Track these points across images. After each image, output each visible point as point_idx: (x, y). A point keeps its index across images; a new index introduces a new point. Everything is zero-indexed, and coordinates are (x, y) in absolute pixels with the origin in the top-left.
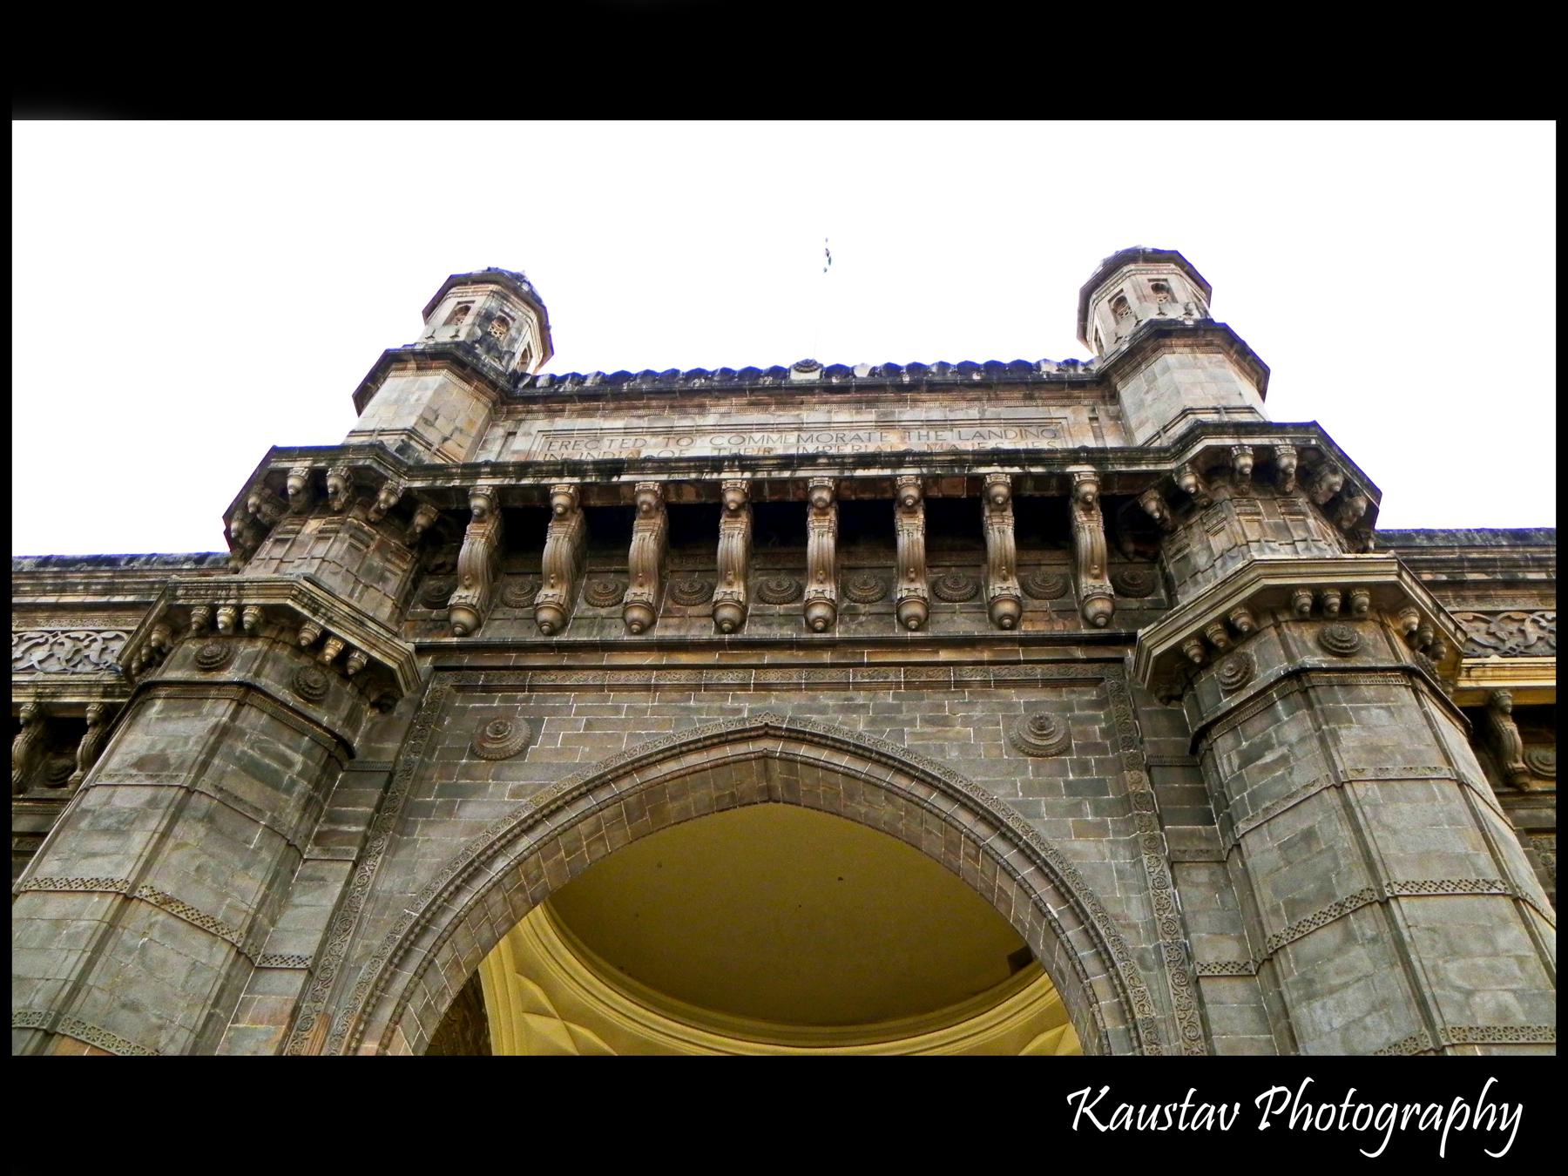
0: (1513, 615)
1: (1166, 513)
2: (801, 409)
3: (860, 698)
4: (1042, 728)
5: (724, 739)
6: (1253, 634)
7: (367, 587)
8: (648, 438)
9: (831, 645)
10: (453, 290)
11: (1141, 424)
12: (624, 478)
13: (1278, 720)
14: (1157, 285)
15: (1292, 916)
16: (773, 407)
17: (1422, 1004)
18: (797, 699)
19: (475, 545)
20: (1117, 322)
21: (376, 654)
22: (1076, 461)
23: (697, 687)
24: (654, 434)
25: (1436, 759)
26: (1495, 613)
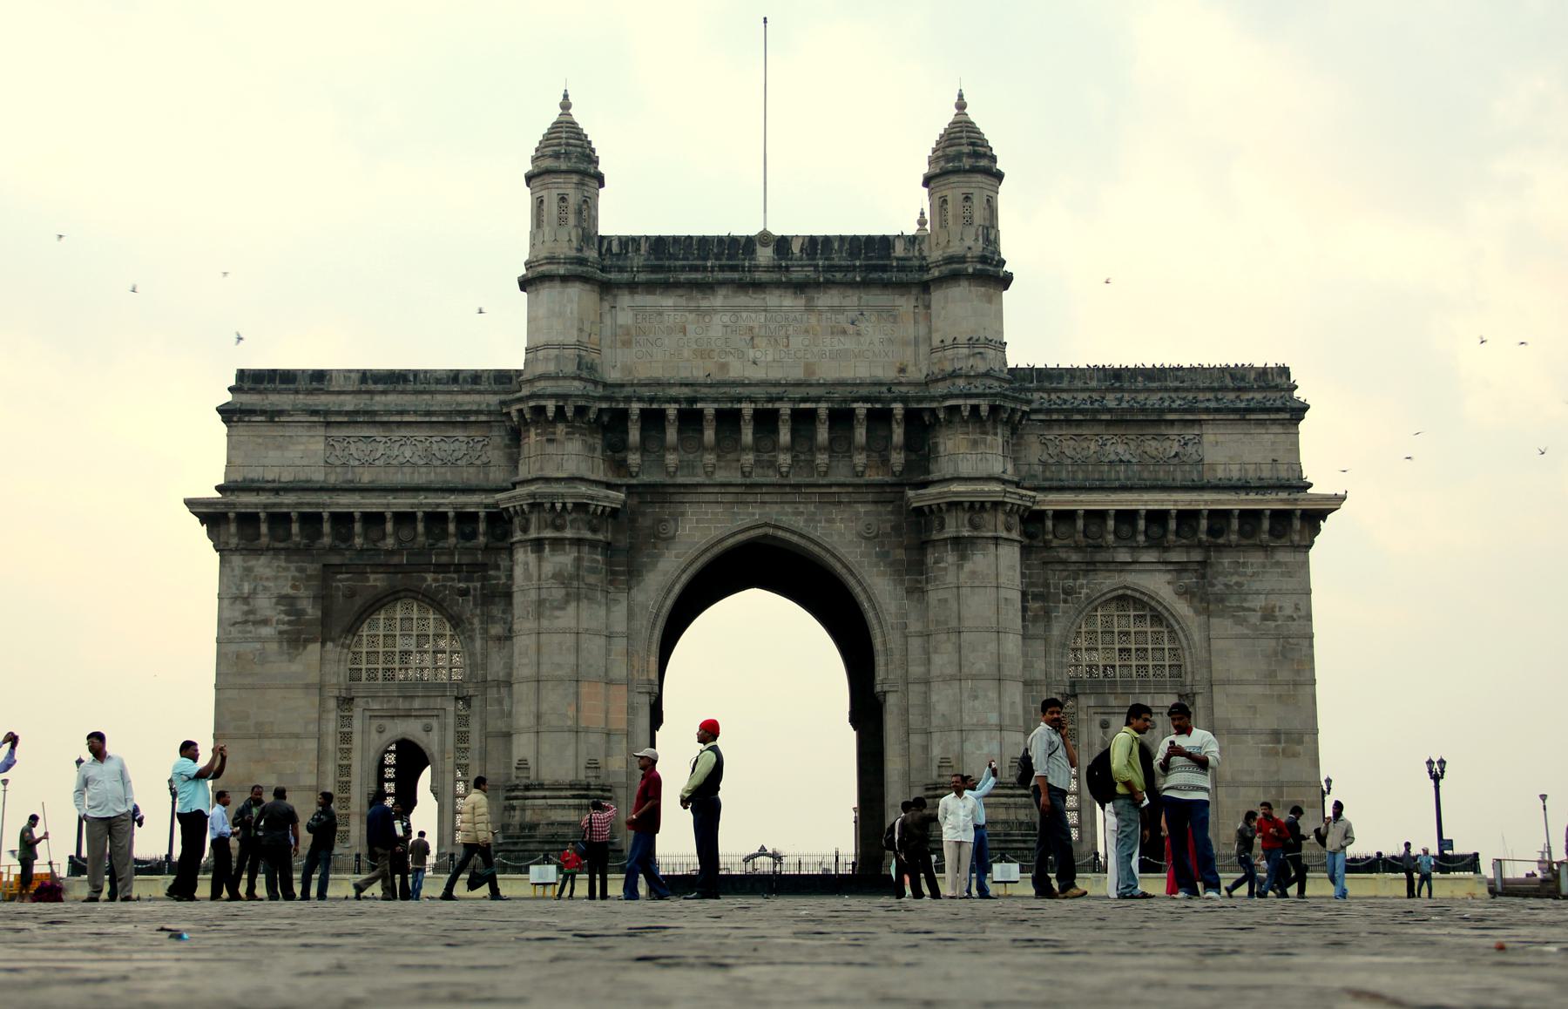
0: (1089, 438)
1: (933, 421)
2: (764, 292)
3: (801, 508)
6: (948, 511)
8: (687, 314)
9: (791, 485)
10: (548, 179)
11: (937, 331)
12: (699, 406)
14: (967, 197)
15: (936, 625)
16: (750, 292)
17: (960, 665)
18: (776, 508)
19: (634, 435)
20: (941, 227)
21: (614, 506)
22: (895, 400)
23: (737, 503)
24: (691, 311)
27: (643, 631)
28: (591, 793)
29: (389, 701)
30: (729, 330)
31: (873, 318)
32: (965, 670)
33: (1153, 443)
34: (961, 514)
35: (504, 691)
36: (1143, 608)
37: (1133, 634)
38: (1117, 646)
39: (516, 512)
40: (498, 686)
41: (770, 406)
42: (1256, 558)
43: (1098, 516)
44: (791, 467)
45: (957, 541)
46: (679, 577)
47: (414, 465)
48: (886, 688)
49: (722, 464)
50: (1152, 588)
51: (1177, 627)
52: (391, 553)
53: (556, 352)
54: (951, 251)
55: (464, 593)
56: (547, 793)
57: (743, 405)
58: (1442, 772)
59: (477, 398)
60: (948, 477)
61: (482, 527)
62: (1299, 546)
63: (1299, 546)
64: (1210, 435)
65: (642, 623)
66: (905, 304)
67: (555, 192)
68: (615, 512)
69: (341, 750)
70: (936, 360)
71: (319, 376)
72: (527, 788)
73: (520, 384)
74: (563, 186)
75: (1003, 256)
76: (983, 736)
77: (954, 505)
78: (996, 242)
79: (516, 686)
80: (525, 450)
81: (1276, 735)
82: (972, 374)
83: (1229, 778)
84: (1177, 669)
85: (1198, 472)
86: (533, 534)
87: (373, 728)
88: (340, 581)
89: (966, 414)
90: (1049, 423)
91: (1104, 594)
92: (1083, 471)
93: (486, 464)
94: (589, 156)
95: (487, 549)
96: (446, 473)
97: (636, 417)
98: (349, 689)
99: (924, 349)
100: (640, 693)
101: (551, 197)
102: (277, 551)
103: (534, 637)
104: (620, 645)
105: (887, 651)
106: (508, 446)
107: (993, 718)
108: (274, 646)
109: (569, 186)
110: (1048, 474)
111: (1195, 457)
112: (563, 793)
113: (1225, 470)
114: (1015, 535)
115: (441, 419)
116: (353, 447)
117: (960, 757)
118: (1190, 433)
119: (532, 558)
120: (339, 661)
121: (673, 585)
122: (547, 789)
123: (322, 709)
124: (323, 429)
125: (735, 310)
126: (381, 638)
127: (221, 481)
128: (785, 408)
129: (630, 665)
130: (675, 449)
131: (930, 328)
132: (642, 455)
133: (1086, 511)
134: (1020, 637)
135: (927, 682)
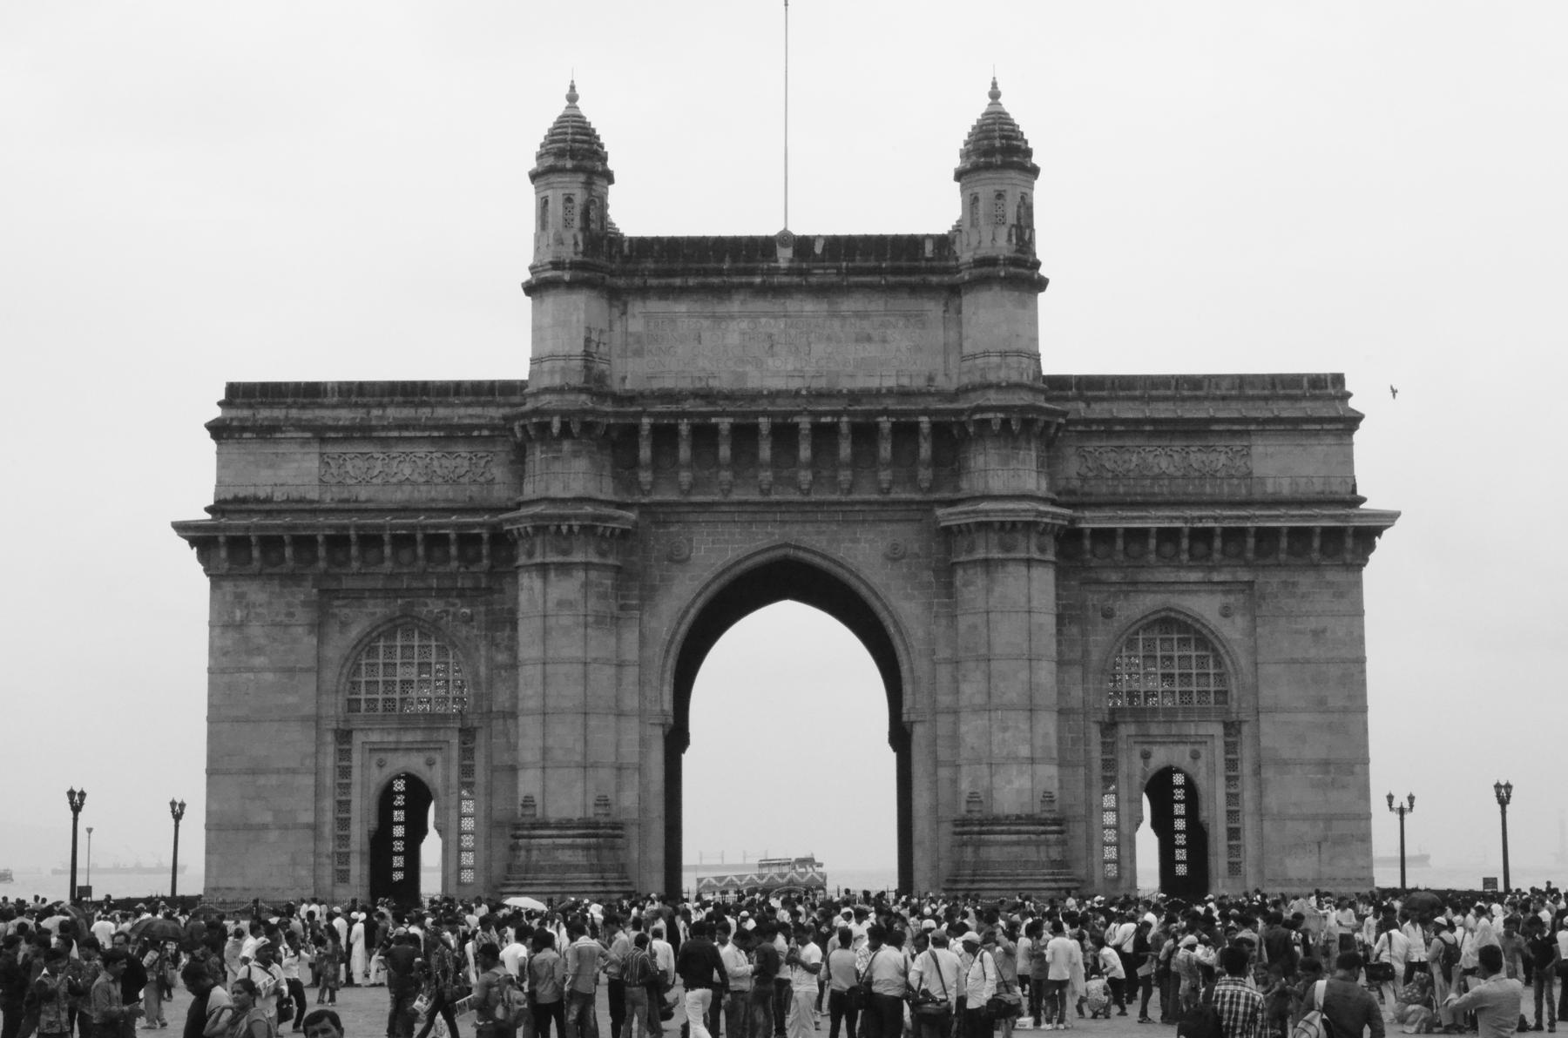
3: (824, 527)
4: (896, 549)
5: (768, 550)
7: (601, 475)
8: (702, 321)
9: (810, 503)
10: (554, 178)
11: (967, 338)
12: (714, 420)
13: (976, 574)
16: (770, 296)
17: (989, 695)
18: (797, 528)
19: (645, 453)
22: (925, 412)
23: (756, 522)
25: (1023, 600)
26: (1122, 447)
27: (656, 659)
28: (601, 832)
29: (389, 734)
30: (747, 337)
31: (901, 324)
33: (1199, 455)
34: (991, 535)
35: (510, 722)
36: (1188, 633)
37: (1176, 660)
39: (520, 534)
40: (504, 717)
41: (789, 420)
42: (1305, 580)
43: (1137, 536)
44: (811, 483)
45: (987, 563)
46: (694, 601)
47: (414, 483)
48: (913, 718)
49: (739, 481)
50: (1196, 609)
51: (1222, 651)
52: (391, 576)
53: (562, 363)
54: (982, 253)
55: (470, 619)
56: (554, 832)
57: (762, 420)
58: (1509, 796)
59: (478, 411)
60: (977, 494)
61: (485, 550)
62: (1351, 565)
63: (1351, 565)
64: (1260, 447)
65: (655, 651)
66: (933, 308)
67: (560, 192)
68: (625, 534)
69: (340, 785)
70: (965, 370)
71: (311, 393)
72: (534, 827)
73: (525, 397)
74: (569, 185)
75: (1039, 257)
76: (1014, 770)
77: (985, 526)
78: (1031, 241)
79: (522, 720)
80: (529, 467)
81: (1325, 764)
82: (1004, 384)
83: (1275, 811)
84: (1223, 696)
85: (1246, 486)
86: (538, 559)
87: (374, 763)
88: (337, 607)
89: (996, 427)
90: (1089, 435)
91: (1146, 617)
92: (1124, 486)
93: (491, 482)
94: (596, 153)
95: (491, 573)
96: (447, 492)
97: (646, 433)
98: (347, 721)
99: (953, 359)
100: (652, 724)
101: (556, 198)
102: (271, 576)
103: (539, 667)
104: (631, 674)
105: (915, 682)
106: (512, 462)
107: (1024, 751)
109: (575, 185)
110: (1086, 489)
111: (1244, 470)
113: (1275, 482)
114: (1050, 556)
115: (442, 434)
116: (349, 467)
117: (990, 792)
118: (1238, 444)
119: (537, 584)
120: (337, 692)
121: (686, 612)
122: (556, 828)
123: (319, 743)
124: (317, 445)
125: (754, 317)
126: (381, 667)
127: (211, 502)
128: (805, 423)
129: (642, 694)
130: (689, 466)
131: (960, 334)
132: (654, 472)
133: (1127, 530)
134: (1054, 665)
135: (956, 712)
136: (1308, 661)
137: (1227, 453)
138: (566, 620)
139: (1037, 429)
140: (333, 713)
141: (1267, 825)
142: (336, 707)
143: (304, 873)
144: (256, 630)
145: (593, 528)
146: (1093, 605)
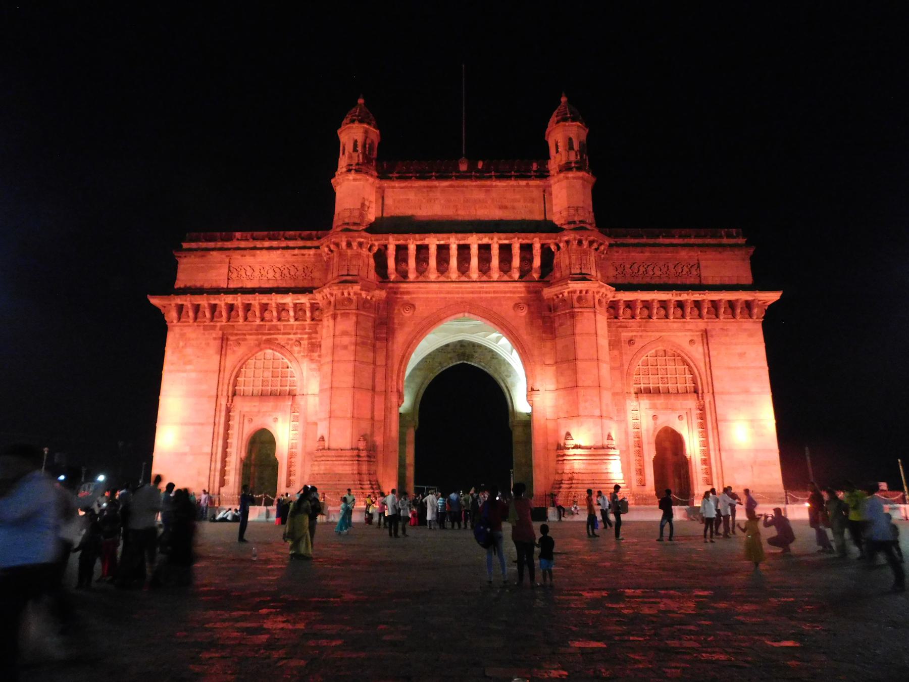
29: (255, 406)
31: (522, 201)
32: (580, 384)
38: (660, 376)
51: (692, 364)
56: (334, 459)
93: (312, 279)
107: (597, 413)
108: (193, 375)
112: (343, 459)
114: (604, 309)
119: (331, 322)
136: (738, 368)
137: (687, 266)
138: (346, 340)
139: (595, 245)
140: (225, 394)
141: (723, 454)
142: (228, 391)
143: (204, 480)
144: (189, 351)
145: (361, 294)
146: (624, 341)
